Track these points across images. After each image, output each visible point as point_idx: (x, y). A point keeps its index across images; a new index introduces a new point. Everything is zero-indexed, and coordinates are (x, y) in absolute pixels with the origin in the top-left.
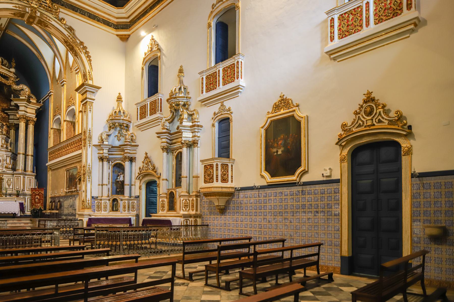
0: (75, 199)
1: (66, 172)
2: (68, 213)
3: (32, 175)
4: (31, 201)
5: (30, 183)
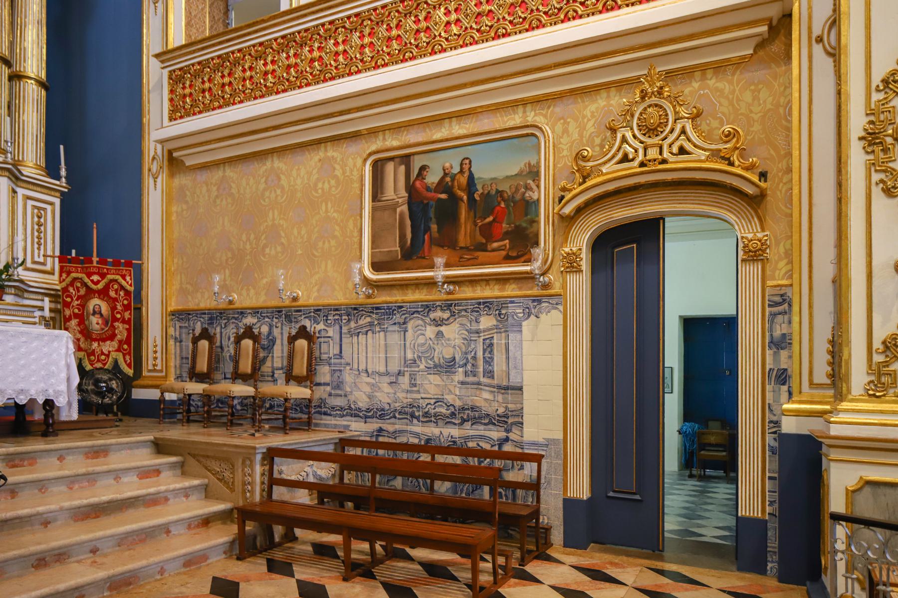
2: (411, 406)
5: (39, 231)
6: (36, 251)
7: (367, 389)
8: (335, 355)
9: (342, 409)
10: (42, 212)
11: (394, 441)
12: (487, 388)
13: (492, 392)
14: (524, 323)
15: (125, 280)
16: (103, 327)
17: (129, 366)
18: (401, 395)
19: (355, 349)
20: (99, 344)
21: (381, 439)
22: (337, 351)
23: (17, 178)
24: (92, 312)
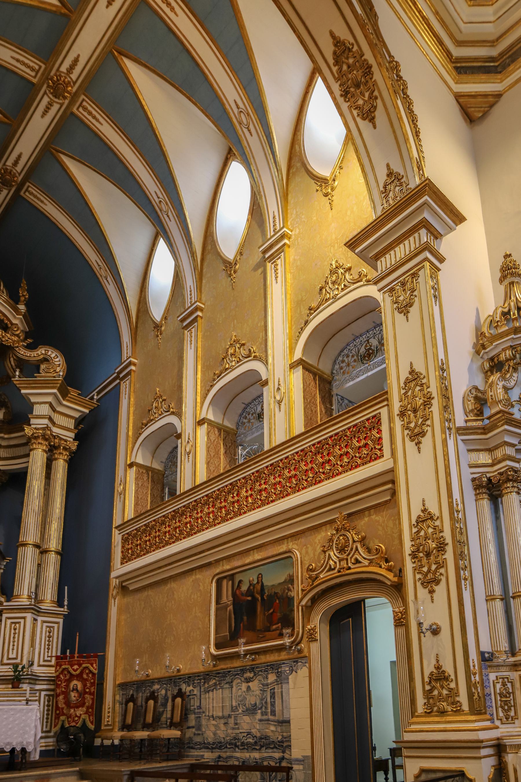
0: (282, 679)
1: (214, 584)
3: (56, 615)
4: (49, 701)
5: (49, 641)
7: (213, 729)
8: (197, 707)
9: (200, 744)
10: (52, 629)
11: (225, 764)
12: (272, 723)
13: (275, 725)
14: (290, 677)
15: (92, 666)
16: (78, 698)
17: (92, 723)
18: (230, 731)
19: (207, 702)
20: (74, 710)
21: (220, 763)
22: (198, 704)
23: (38, 612)
24: (72, 689)
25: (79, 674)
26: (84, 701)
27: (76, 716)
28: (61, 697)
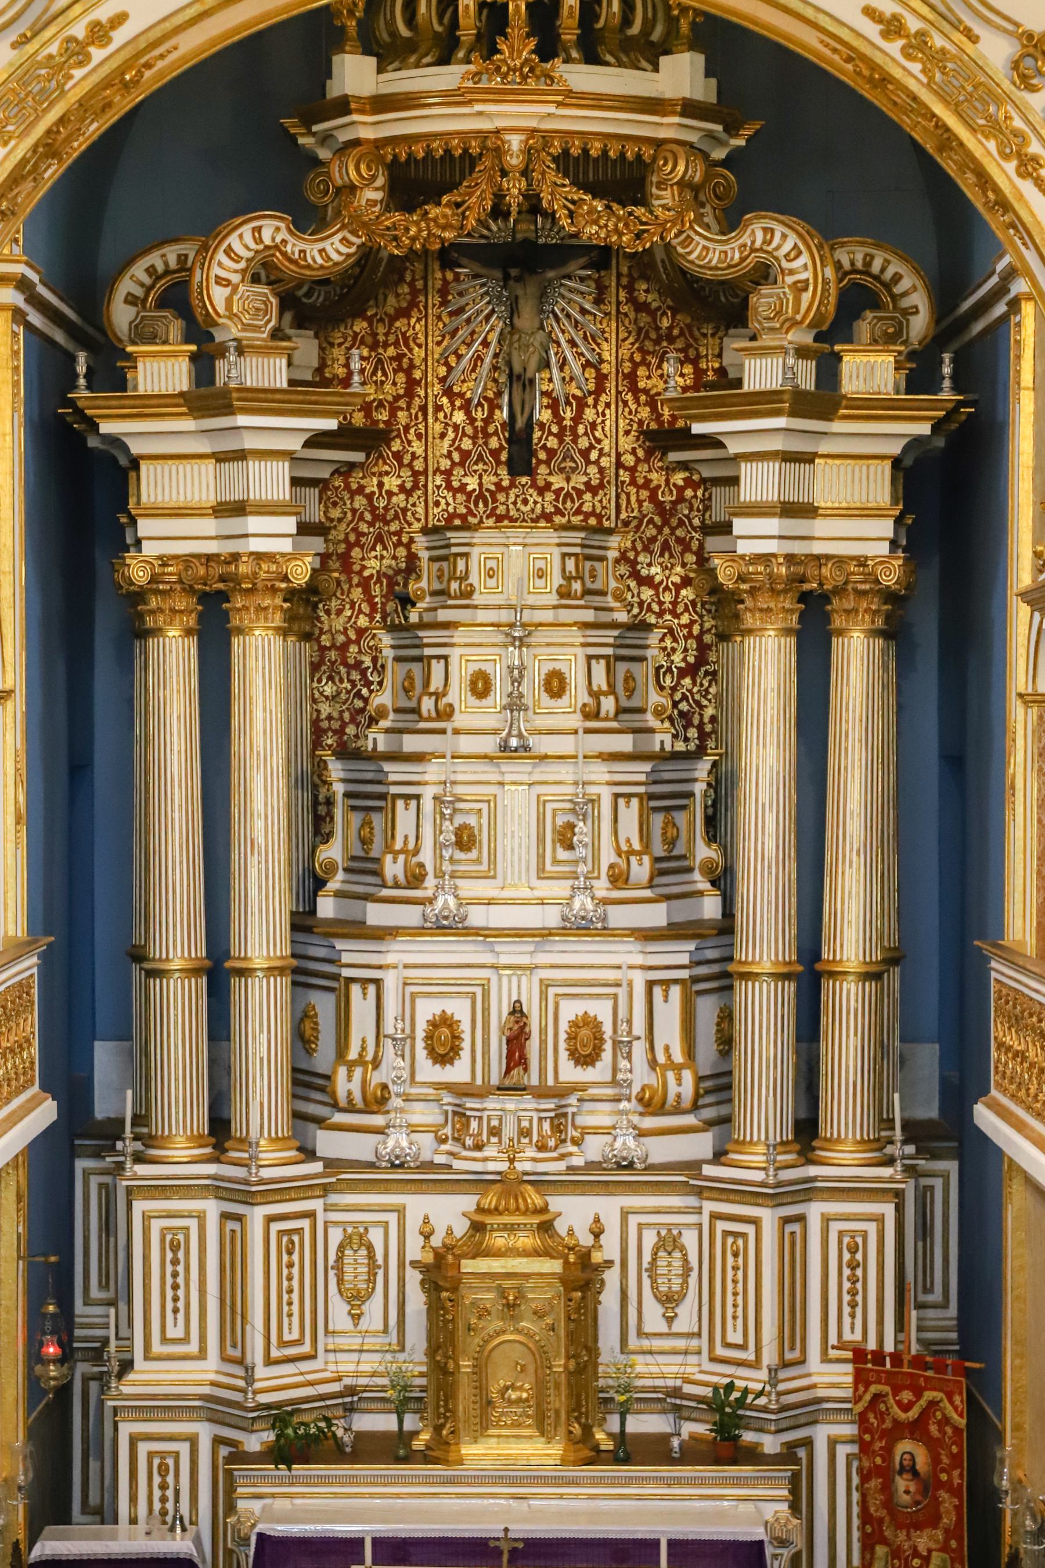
5: (853, 1280)
6: (847, 1320)
16: (919, 1498)
20: (908, 1535)
24: (897, 1467)
25: (917, 1420)
26: (937, 1510)
27: (916, 1554)
28: (875, 1483)
